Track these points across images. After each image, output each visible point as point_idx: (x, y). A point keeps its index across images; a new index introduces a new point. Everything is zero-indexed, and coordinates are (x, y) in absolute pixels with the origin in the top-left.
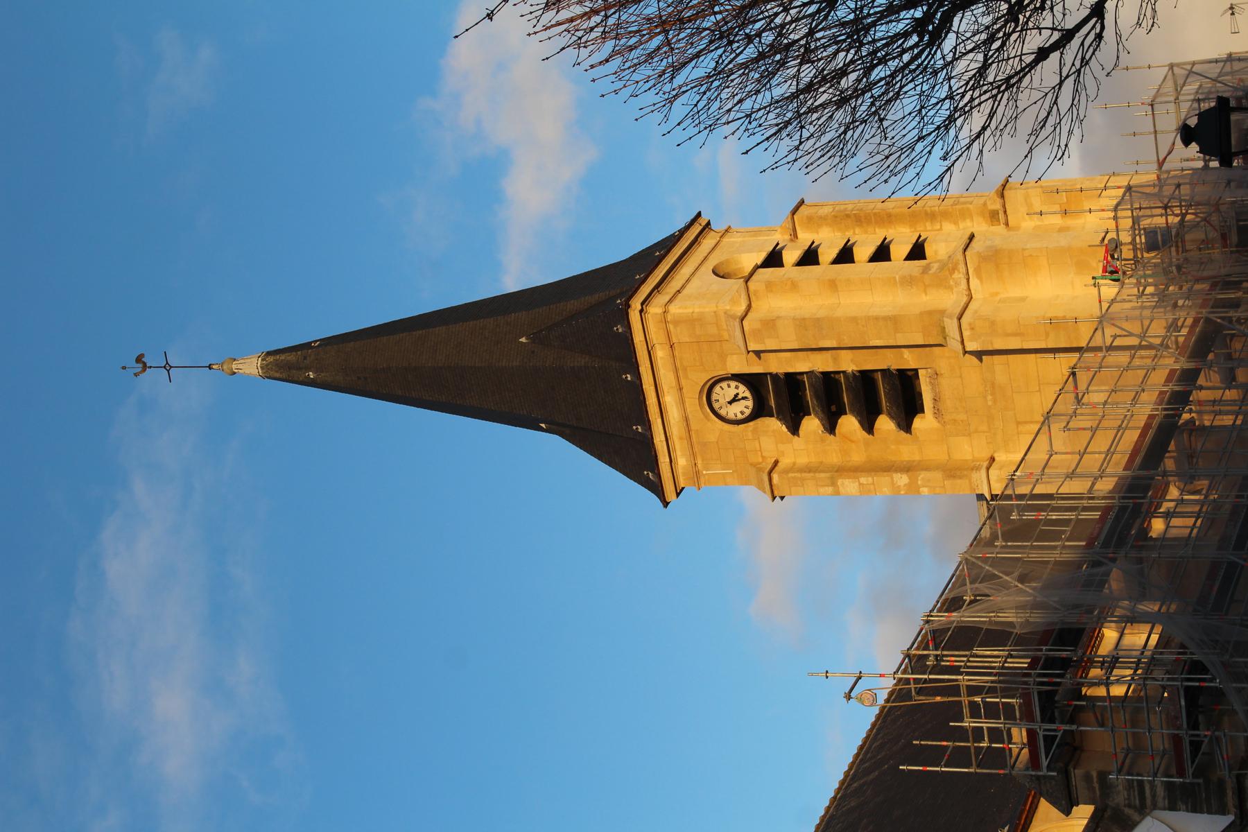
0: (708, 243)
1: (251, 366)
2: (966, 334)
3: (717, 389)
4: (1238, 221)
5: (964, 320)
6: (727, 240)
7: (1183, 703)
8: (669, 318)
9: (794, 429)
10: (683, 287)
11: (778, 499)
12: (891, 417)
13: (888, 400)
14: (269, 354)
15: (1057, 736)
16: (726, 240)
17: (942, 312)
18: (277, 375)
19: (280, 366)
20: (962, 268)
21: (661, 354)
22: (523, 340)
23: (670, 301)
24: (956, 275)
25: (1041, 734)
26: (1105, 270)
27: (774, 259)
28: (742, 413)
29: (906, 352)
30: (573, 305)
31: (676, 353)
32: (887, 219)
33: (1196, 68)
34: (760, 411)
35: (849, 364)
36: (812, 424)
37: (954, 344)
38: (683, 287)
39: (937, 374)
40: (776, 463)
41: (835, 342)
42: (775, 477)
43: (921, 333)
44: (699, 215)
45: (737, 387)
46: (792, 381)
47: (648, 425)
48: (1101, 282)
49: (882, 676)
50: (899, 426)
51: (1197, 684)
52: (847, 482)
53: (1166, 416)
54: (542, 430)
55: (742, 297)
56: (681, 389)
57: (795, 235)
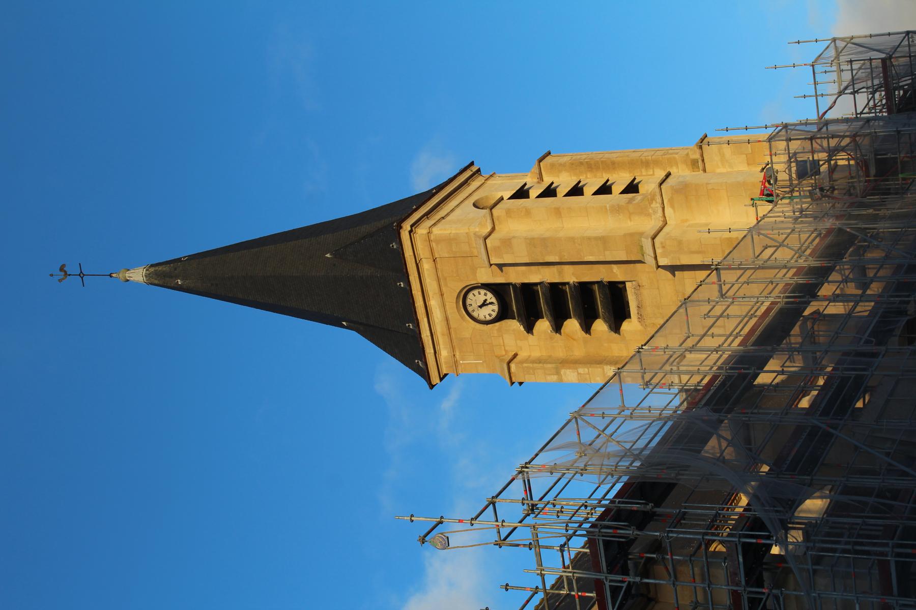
0: (475, 184)
1: (138, 275)
2: (658, 251)
3: (470, 295)
4: (876, 155)
5: (656, 240)
6: (491, 182)
7: (741, 559)
8: (432, 237)
9: (529, 329)
10: (448, 215)
11: (516, 384)
12: (605, 321)
13: (603, 308)
14: (152, 266)
15: (623, 587)
16: (490, 182)
17: (641, 234)
18: (156, 282)
19: (157, 275)
20: (659, 199)
21: (426, 266)
22: (328, 255)
23: (434, 224)
24: (654, 205)
25: (607, 584)
26: (762, 193)
27: (522, 193)
28: (490, 315)
29: (615, 267)
30: (365, 229)
31: (439, 266)
32: (612, 166)
33: (854, 41)
34: (504, 314)
35: (571, 276)
36: (543, 325)
37: (650, 260)
38: (448, 215)
39: (639, 286)
40: (515, 355)
41: (557, 258)
42: (513, 366)
43: (625, 251)
44: (472, 164)
45: (485, 295)
46: (527, 290)
47: (417, 324)
48: (758, 202)
49: (461, 521)
50: (611, 328)
51: (754, 541)
52: (568, 371)
53: (787, 303)
54: (343, 326)
55: (488, 221)
56: (442, 295)
57: (541, 178)
